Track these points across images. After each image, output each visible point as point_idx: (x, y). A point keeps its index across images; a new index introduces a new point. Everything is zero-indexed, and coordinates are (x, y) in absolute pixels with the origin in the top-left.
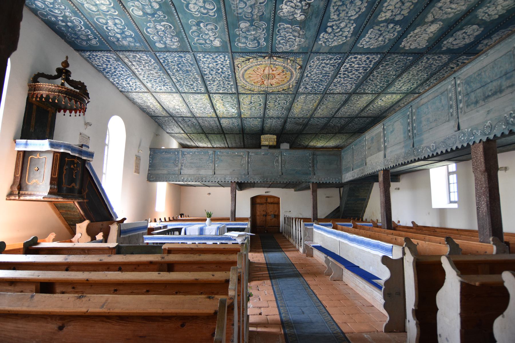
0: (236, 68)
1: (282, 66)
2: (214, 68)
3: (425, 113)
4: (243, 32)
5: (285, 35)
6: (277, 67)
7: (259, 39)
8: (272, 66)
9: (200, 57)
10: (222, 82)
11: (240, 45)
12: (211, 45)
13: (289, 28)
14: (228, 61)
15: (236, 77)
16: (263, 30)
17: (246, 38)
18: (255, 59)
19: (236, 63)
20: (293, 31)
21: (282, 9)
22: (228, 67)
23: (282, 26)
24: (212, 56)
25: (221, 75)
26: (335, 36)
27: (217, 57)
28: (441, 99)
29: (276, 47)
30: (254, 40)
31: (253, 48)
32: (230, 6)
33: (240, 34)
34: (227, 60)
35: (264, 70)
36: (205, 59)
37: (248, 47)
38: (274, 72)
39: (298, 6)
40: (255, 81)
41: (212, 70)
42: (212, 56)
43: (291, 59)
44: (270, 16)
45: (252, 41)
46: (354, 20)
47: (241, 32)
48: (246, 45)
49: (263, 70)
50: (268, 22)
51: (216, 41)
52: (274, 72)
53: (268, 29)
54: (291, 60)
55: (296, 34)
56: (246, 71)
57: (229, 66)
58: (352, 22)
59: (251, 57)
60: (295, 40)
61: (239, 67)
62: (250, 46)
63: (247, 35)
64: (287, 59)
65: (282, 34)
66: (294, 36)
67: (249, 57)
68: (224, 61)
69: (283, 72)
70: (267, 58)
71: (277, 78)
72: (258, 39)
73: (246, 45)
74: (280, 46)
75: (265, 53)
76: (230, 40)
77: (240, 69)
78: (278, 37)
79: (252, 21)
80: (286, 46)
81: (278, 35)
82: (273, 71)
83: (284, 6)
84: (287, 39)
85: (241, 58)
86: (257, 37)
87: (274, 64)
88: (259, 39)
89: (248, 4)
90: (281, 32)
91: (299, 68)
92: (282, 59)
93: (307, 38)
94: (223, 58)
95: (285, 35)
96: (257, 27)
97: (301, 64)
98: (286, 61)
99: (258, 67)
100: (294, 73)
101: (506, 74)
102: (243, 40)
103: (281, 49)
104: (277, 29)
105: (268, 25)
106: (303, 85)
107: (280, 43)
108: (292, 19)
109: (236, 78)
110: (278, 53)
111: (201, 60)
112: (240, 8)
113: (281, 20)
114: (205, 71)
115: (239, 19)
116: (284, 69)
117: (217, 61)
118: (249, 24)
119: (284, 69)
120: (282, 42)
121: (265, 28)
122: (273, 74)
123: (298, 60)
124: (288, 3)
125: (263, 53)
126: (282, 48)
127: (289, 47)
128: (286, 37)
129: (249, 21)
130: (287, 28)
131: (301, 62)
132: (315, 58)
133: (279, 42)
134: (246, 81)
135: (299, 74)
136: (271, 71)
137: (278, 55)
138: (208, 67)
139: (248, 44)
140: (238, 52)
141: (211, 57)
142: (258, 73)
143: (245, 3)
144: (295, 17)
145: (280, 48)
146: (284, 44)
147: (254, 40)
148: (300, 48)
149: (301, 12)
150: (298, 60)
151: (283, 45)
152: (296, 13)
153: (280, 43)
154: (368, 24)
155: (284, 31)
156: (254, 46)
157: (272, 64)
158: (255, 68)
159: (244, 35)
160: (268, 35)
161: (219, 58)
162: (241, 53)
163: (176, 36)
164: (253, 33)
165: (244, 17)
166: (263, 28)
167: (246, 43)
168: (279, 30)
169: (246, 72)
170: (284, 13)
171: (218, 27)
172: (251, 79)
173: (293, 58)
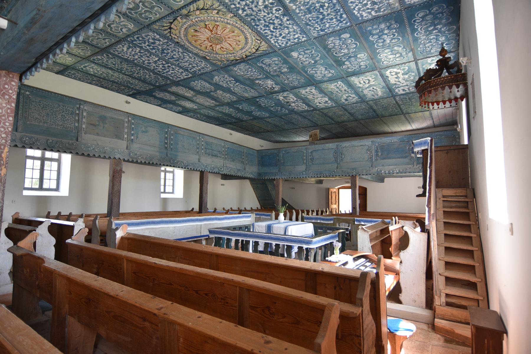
2: (280, 28)
3: (182, 140)
9: (303, 37)
10: (254, 9)
12: (298, 51)
14: (273, 42)
18: (252, 52)
22: (267, 36)
24: (292, 42)
25: (265, 22)
27: (287, 43)
28: (193, 141)
31: (264, 60)
35: (230, 45)
36: (296, 36)
41: (281, 25)
42: (292, 42)
49: (231, 44)
57: (268, 37)
60: (244, 73)
67: (259, 52)
68: (277, 41)
71: (206, 42)
85: (265, 49)
101: (219, 152)
111: (300, 34)
114: (288, 20)
117: (283, 39)
127: (240, 68)
138: (288, 28)
141: (292, 41)
161: (285, 43)
163: (331, 49)
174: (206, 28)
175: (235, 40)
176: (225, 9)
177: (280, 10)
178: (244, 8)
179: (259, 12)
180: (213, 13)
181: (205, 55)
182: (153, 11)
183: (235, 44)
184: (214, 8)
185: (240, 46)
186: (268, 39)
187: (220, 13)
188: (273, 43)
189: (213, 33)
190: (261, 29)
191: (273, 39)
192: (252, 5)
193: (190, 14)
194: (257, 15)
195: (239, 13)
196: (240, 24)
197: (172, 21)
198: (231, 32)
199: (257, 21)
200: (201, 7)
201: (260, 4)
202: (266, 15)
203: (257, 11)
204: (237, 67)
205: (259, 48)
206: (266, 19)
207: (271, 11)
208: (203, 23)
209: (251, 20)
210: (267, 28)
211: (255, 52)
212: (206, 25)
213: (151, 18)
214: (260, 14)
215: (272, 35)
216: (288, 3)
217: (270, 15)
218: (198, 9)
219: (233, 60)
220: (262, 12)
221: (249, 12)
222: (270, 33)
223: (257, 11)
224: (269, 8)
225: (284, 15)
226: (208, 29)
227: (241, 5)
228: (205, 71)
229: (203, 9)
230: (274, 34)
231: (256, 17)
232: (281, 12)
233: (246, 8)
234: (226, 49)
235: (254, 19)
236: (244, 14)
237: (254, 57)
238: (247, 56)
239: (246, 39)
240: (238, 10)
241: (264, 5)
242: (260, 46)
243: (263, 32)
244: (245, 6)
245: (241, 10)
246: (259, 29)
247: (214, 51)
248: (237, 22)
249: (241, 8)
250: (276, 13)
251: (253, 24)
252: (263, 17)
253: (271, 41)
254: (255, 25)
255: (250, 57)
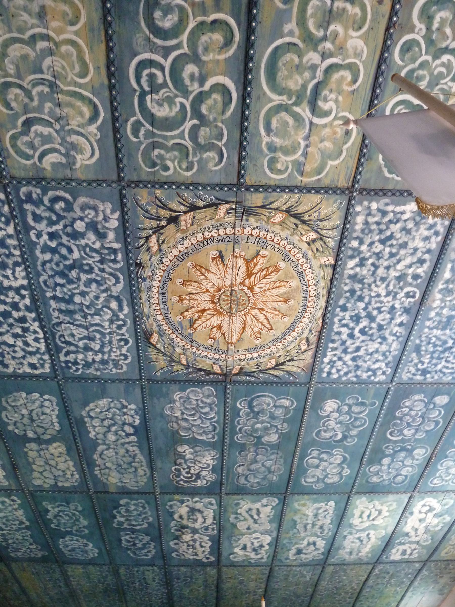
0: (313, 339)
1: (199, 345)
2: (372, 335)
4: (276, 426)
5: (202, 422)
6: (210, 342)
7: (248, 414)
8: (223, 347)
10: (381, 272)
11: (286, 403)
13: (198, 434)
14: (326, 360)
15: (327, 301)
16: (240, 429)
17: (273, 417)
18: (263, 367)
19: (310, 354)
20: (190, 429)
21: (213, 459)
23: (210, 436)
25: (365, 309)
26: (112, 419)
27: (346, 374)
29: (216, 396)
30: (258, 413)
32: (285, 462)
33: (282, 424)
34: (328, 364)
35: (244, 328)
37: (272, 398)
38: (215, 321)
39: (191, 462)
40: (273, 277)
43: (180, 367)
44: (229, 451)
45: (262, 411)
46: (99, 444)
47: (279, 427)
48: (275, 402)
49: (247, 329)
50: (233, 444)
51: (330, 409)
52: (215, 321)
53: (233, 432)
54: (179, 363)
55: (184, 424)
56: (292, 328)
57: (331, 345)
58: (100, 441)
59: (271, 372)
60: (183, 413)
61: (307, 340)
62: (268, 400)
63: (269, 423)
64: (188, 367)
65: (208, 424)
66: (186, 420)
67: (276, 372)
68: (334, 362)
69: (192, 323)
70: (235, 371)
71: (206, 296)
72: (252, 415)
73: (275, 402)
74: (208, 401)
75: (239, 383)
76: (303, 413)
77: (305, 335)
78: (214, 417)
79: (258, 442)
80: (197, 400)
81: (215, 422)
82: (219, 327)
83: (211, 462)
84: (198, 415)
85: (295, 369)
86: (253, 418)
87: (217, 351)
88: (248, 414)
89: (260, 465)
90: (210, 427)
91: (151, 334)
92: (200, 366)
93: (162, 415)
94: (334, 371)
95: (202, 422)
96: (251, 435)
97: (151, 350)
98: (190, 359)
99: (257, 342)
100: (160, 317)
102: (279, 412)
103: (206, 393)
104: (217, 431)
105: (232, 438)
106: (115, 251)
107: (210, 405)
108: (196, 446)
109: (329, 292)
110: (211, 383)
112: (272, 460)
113: (213, 446)
115: (277, 447)
116: (191, 335)
118: (263, 439)
119: (191, 335)
120: (207, 410)
121: (238, 433)
122: (219, 313)
123: (162, 364)
124: (205, 466)
125: (244, 383)
126: (204, 396)
127: (191, 396)
128: (200, 418)
129: (263, 444)
130: (201, 434)
131: (154, 357)
132: (125, 368)
133: (211, 409)
134: (301, 275)
135: (146, 310)
136: (225, 329)
137: (211, 376)
139: (272, 405)
140: (296, 384)
142: (262, 317)
143: (263, 465)
144: (192, 448)
145: (208, 396)
146: (202, 405)
147: (258, 413)
148: (168, 394)
149: (185, 456)
150: (162, 364)
151: (202, 402)
152: (192, 454)
153: (210, 405)
154: (72, 438)
155: (206, 430)
156: (260, 398)
157: (223, 352)
158: (269, 336)
159: (275, 423)
160: (232, 421)
162: (291, 383)
163: (395, 418)
164: (259, 426)
165: (269, 449)
166: (241, 433)
167: (275, 406)
168: (214, 431)
169: (292, 322)
170: (210, 454)
171: (314, 434)
172: (283, 290)
173: (175, 368)
174: (248, 262)
175: (266, 321)
176: (335, 241)
177: (413, 297)
178: (367, 259)
179: (378, 283)
180: (304, 238)
181: (155, 328)
182: (195, 154)
183: (256, 330)
184: (321, 227)
185: (257, 342)
186: (327, 347)
187: (318, 244)
188: (323, 362)
189: (247, 282)
190: (340, 321)
191: (334, 352)
192: (386, 260)
193: (259, 211)
194: (370, 285)
195: (346, 264)
196: (320, 290)
197: (201, 204)
198: (281, 299)
199: (356, 297)
200: (300, 210)
201: (399, 267)
202: (383, 293)
203: (378, 279)
204: (188, 391)
205: (287, 363)
206: (373, 302)
207: (400, 291)
208: (257, 248)
209: (346, 292)
210: (352, 325)
211: (267, 370)
212: (257, 254)
213: (166, 169)
214: (377, 286)
215: (344, 343)
216: (437, 290)
217: (390, 298)
218: (287, 211)
219: (200, 370)
220: (384, 285)
221: (365, 272)
222: (344, 337)
223: (378, 279)
224: (402, 283)
225: (407, 311)
226: (248, 267)
227: (369, 251)
228: (99, 373)
229: (296, 216)
230: (348, 343)
231: (361, 290)
232: (410, 302)
233: (370, 261)
234: (224, 334)
235: (352, 292)
236: (351, 272)
237: (252, 379)
238: (242, 372)
239: (290, 329)
240: (352, 257)
241: (403, 272)
242: (295, 359)
243: (336, 330)
244: (374, 256)
245: (357, 260)
246: (336, 320)
247: (191, 326)
248: (321, 281)
249: (362, 256)
250: (400, 300)
251: (341, 302)
252: (373, 294)
253: (325, 356)
254: (340, 307)
255: (244, 378)
